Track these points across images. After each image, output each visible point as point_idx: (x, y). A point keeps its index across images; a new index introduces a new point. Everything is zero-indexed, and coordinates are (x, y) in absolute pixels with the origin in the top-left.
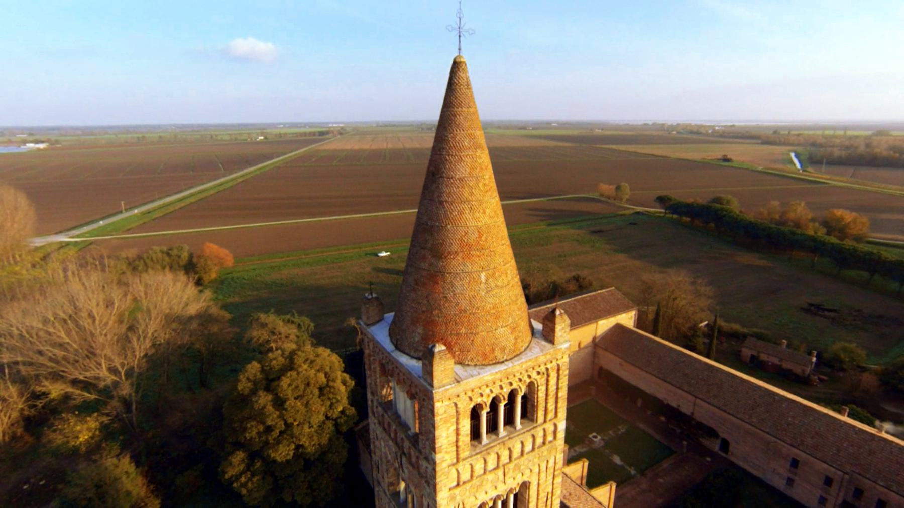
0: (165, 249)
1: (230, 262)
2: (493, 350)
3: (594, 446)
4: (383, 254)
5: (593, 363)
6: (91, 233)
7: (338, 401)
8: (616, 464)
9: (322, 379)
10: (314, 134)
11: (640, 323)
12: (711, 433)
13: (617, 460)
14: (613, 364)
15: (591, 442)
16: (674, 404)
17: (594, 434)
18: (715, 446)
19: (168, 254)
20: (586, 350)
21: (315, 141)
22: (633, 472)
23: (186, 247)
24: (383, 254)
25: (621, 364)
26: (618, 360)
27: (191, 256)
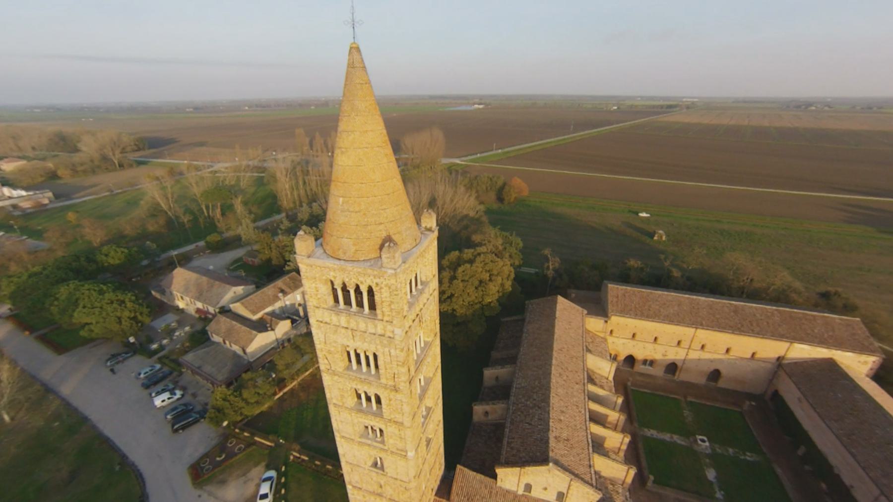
0: (491, 176)
3: (695, 447)
4: (644, 215)
5: (771, 381)
6: (472, 161)
7: (488, 295)
8: (706, 477)
9: (486, 276)
10: (662, 107)
13: (711, 474)
14: (791, 394)
15: (696, 441)
17: (705, 438)
20: (763, 365)
21: (659, 113)
22: (719, 495)
24: (644, 215)
25: (799, 399)
26: (798, 394)
27: (505, 184)
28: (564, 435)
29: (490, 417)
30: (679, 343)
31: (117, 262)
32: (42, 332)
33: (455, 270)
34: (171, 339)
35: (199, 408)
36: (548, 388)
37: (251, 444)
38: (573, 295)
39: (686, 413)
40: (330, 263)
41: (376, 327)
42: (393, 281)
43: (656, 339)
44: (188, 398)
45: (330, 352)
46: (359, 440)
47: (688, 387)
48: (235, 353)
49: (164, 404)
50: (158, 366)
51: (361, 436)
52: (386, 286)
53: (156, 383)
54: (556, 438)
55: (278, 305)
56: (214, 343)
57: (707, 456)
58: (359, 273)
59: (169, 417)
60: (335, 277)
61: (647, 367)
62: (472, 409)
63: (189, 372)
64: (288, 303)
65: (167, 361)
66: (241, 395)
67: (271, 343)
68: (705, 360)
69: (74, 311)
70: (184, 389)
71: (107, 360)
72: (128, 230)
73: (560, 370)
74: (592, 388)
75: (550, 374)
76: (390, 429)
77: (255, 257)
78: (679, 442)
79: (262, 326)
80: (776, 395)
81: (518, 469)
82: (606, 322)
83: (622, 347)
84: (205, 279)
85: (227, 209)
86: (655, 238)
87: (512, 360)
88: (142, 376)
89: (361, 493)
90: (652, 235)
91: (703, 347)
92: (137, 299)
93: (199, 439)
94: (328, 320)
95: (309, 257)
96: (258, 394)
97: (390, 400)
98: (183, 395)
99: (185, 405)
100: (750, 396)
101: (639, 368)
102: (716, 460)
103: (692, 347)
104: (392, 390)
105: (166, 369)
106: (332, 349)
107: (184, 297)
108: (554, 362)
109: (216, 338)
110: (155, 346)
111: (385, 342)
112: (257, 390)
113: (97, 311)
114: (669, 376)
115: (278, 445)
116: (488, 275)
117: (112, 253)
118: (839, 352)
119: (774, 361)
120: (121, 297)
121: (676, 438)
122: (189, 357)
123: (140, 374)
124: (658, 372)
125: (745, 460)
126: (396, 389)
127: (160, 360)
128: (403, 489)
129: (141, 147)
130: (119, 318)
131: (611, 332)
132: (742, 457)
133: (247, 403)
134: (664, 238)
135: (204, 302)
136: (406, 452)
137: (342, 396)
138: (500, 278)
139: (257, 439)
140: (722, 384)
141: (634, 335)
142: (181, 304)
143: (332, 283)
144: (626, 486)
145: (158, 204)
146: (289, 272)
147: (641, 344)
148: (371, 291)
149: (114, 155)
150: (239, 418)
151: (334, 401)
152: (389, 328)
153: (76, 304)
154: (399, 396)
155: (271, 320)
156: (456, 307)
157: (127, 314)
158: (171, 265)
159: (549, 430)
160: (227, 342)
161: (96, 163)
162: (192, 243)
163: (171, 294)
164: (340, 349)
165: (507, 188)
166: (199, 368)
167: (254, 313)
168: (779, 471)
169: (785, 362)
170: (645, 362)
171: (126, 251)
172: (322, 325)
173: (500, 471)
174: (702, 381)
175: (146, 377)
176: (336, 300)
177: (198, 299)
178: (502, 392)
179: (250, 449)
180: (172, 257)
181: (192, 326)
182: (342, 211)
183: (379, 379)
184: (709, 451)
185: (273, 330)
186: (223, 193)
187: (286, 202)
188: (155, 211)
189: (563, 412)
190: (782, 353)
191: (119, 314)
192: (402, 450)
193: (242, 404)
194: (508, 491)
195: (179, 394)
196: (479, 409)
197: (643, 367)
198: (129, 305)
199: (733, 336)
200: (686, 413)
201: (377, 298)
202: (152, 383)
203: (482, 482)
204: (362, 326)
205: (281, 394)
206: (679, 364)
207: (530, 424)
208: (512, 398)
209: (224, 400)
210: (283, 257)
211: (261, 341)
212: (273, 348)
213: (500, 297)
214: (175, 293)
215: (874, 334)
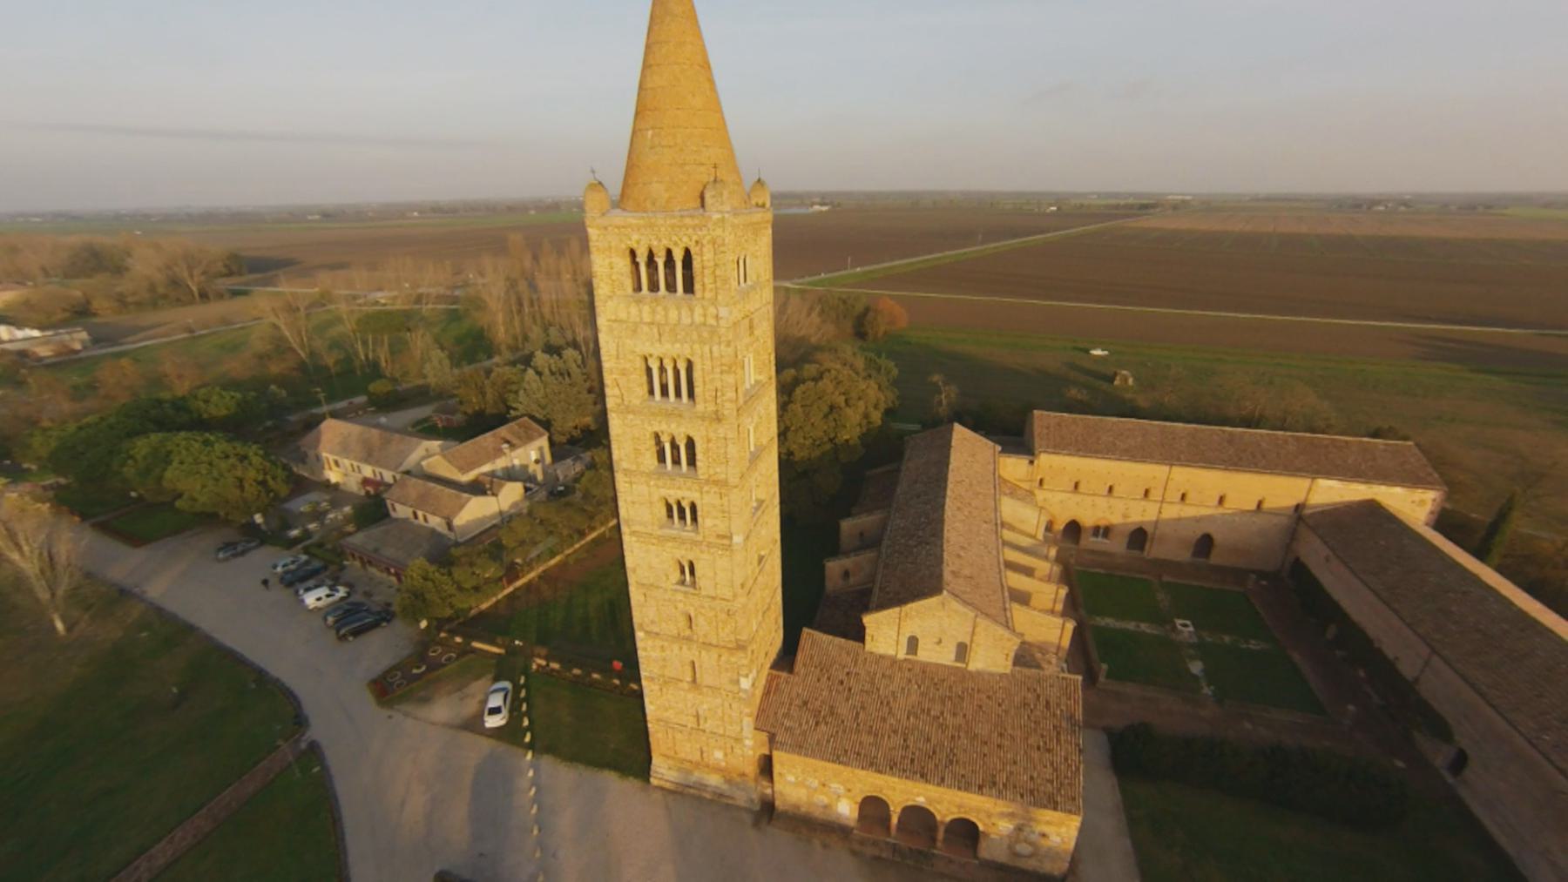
3: (1174, 636)
4: (1097, 352)
5: (1288, 547)
6: (809, 284)
8: (1187, 669)
9: (841, 400)
10: (1131, 207)
12: (1442, 731)
13: (1196, 667)
14: (1314, 554)
15: (1174, 628)
16: (1390, 654)
18: (1440, 758)
19: (844, 302)
20: (1275, 520)
21: (1128, 216)
24: (1097, 352)
25: (1327, 559)
27: (867, 310)
28: (966, 572)
29: (852, 580)
30: (1147, 493)
31: (224, 412)
32: (101, 518)
33: (790, 395)
34: (322, 524)
36: (941, 521)
37: (465, 651)
39: (1160, 596)
41: (692, 310)
42: (719, 232)
43: (1111, 489)
44: (356, 598)
45: (624, 373)
46: (659, 533)
47: (1163, 565)
48: (433, 531)
49: (320, 604)
50: (304, 558)
51: (661, 527)
53: (303, 579)
54: (953, 572)
55: (500, 464)
57: (1192, 646)
58: (673, 226)
59: (330, 619)
62: (823, 567)
63: (357, 563)
64: (517, 462)
66: (450, 574)
67: (492, 517)
69: (165, 470)
70: (346, 585)
71: (220, 550)
75: (943, 506)
76: (707, 499)
77: (453, 412)
79: (478, 488)
80: (1299, 569)
81: (897, 609)
82: (1031, 462)
84: (375, 432)
86: (1117, 382)
88: (279, 569)
89: (659, 643)
90: (1111, 379)
91: (1183, 497)
93: (381, 649)
94: (623, 316)
97: (709, 441)
98: (349, 594)
100: (1262, 574)
101: (1089, 541)
105: (316, 564)
107: (340, 461)
108: (949, 493)
109: (402, 512)
110: (295, 533)
111: (705, 335)
113: (204, 469)
114: (1136, 553)
115: (512, 651)
116: (843, 398)
117: (215, 398)
118: (1383, 488)
119: (1291, 512)
121: (1144, 627)
123: (275, 567)
124: (1117, 546)
126: (718, 418)
127: (306, 551)
128: (723, 616)
129: (234, 268)
130: (241, 480)
131: (1041, 481)
133: (460, 589)
134: (1131, 381)
136: (731, 538)
138: (861, 403)
139: (476, 645)
140: (1215, 559)
141: (1076, 486)
142: (333, 476)
143: (633, 253)
144: (1063, 654)
145: (282, 339)
146: (517, 418)
147: (1089, 500)
149: (191, 276)
150: (448, 612)
151: (625, 465)
153: (167, 460)
155: (492, 483)
156: (794, 447)
157: (252, 474)
160: (420, 514)
161: (161, 290)
162: (342, 399)
163: (318, 458)
165: (871, 315)
166: (376, 550)
167: (463, 470)
168: (1296, 657)
169: (1307, 512)
170: (1096, 530)
171: (238, 395)
172: (615, 325)
173: (869, 620)
174: (1185, 556)
175: (286, 573)
176: (638, 288)
177: (368, 458)
178: (868, 542)
179: (464, 660)
184: (1195, 640)
186: (396, 324)
187: (501, 334)
188: (280, 347)
189: (963, 548)
190: (1300, 498)
191: (239, 473)
192: (723, 537)
194: (882, 657)
195: (342, 592)
196: (834, 567)
197: (1093, 539)
198: (256, 460)
199: (1227, 474)
200: (1160, 596)
201: (696, 264)
202: (297, 580)
203: (841, 648)
204: (673, 314)
205: (511, 589)
206: (1149, 529)
210: (504, 401)
211: (475, 511)
212: (494, 526)
214: (324, 455)
215: (1434, 467)
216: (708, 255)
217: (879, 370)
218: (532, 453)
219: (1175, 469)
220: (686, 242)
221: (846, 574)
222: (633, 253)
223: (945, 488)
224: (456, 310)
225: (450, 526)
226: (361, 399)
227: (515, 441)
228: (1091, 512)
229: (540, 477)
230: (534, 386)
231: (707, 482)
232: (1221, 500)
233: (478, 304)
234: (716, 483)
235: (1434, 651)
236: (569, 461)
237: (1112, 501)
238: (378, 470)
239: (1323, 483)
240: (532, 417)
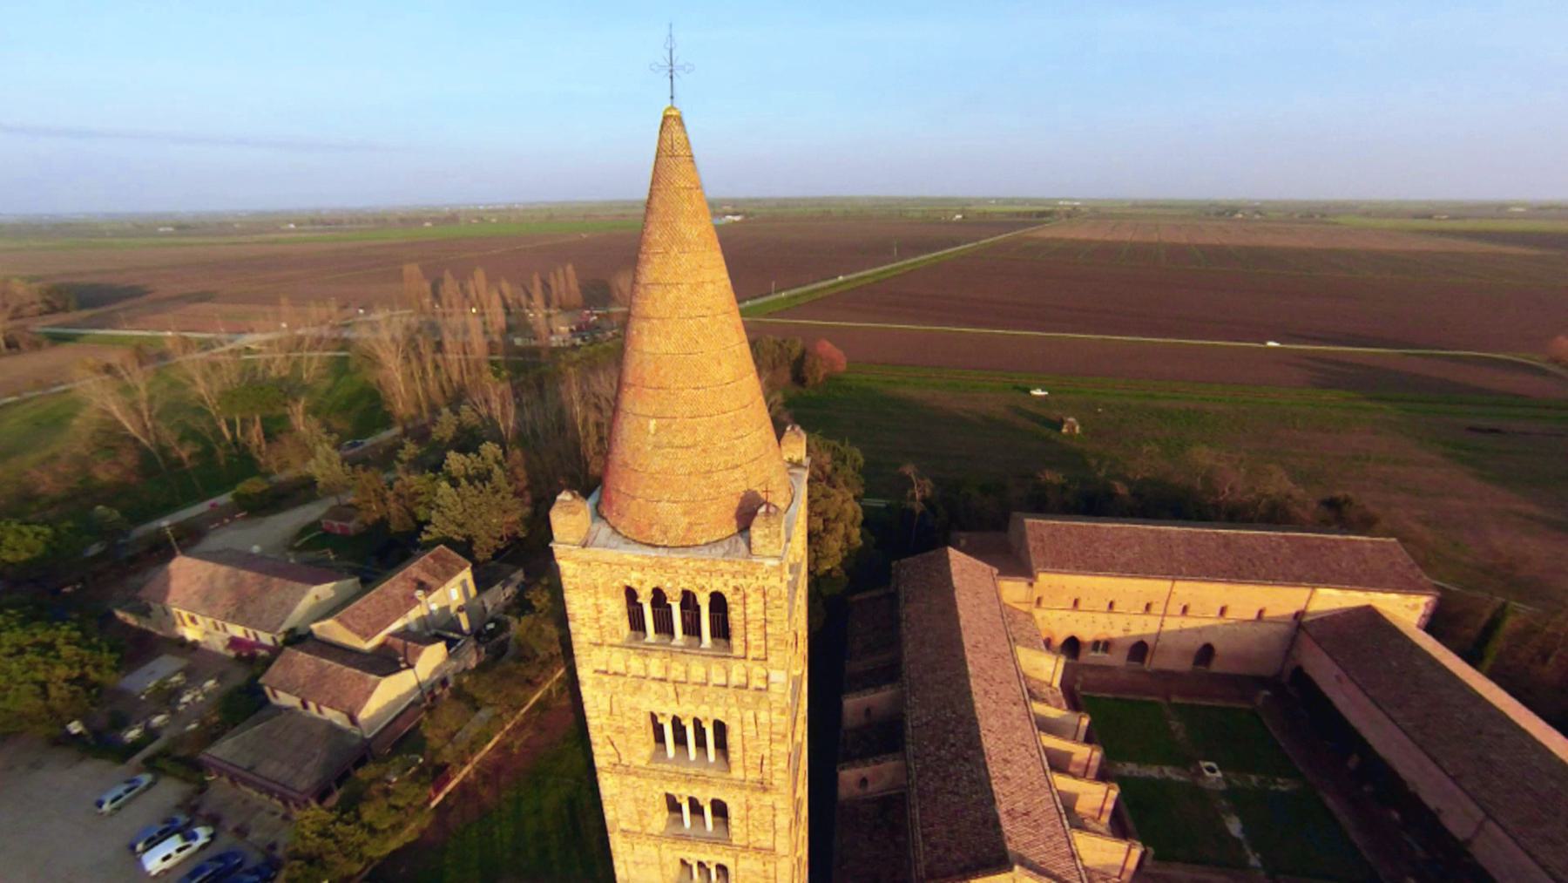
0: (779, 339)
1: (842, 366)
2: (651, 525)
4: (1038, 392)
7: (825, 557)
8: (1226, 831)
10: (1030, 214)
11: (1433, 625)
13: (1234, 826)
14: (1323, 670)
15: (1200, 772)
17: (1214, 765)
20: (1274, 627)
22: (1254, 861)
23: (800, 342)
24: (1038, 392)
26: (1336, 670)
27: (804, 352)
28: (1020, 807)
29: (870, 788)
30: (1148, 607)
31: (24, 556)
34: (174, 712)
35: (255, 859)
36: (974, 722)
38: (963, 542)
39: (1175, 725)
40: (632, 554)
43: (1111, 605)
44: (226, 841)
45: (620, 730)
48: (331, 727)
52: (756, 590)
54: (1008, 813)
55: (414, 614)
56: (280, 710)
58: (698, 571)
60: (642, 583)
61: (1100, 654)
62: (836, 776)
63: (225, 780)
65: (161, 763)
66: (358, 817)
67: (409, 694)
68: (1189, 630)
70: (214, 821)
72: (47, 484)
73: (984, 684)
74: (1038, 708)
76: (743, 864)
77: (349, 518)
78: (1175, 777)
79: (387, 661)
80: (1301, 678)
82: (1031, 585)
83: (1059, 623)
85: (275, 429)
86: (1064, 430)
87: (890, 673)
90: (1058, 425)
91: (1185, 609)
92: (86, 637)
94: (621, 668)
95: (584, 546)
96: (396, 807)
97: (749, 809)
98: (212, 837)
99: (220, 858)
100: (1261, 681)
101: (1088, 657)
102: (1238, 800)
103: (1169, 611)
104: (754, 790)
106: (627, 724)
107: (198, 618)
110: (133, 734)
111: (749, 699)
112: (392, 801)
118: (1379, 595)
119: (1290, 620)
120: (43, 635)
121: (1168, 771)
122: (223, 749)
123: (100, 804)
124: (1117, 659)
125: (1277, 791)
126: (764, 787)
127: (150, 764)
129: (59, 304)
130: (43, 686)
131: (1039, 601)
132: (1273, 788)
133: (373, 830)
135: (246, 623)
137: (642, 814)
138: (841, 526)
140: (1216, 667)
141: (1076, 603)
142: (191, 633)
148: (718, 602)
151: (623, 825)
152: (758, 670)
154: (768, 799)
155: (405, 648)
157: (61, 671)
158: (161, 551)
159: (994, 800)
160: (312, 705)
162: (203, 500)
163: (167, 613)
164: (642, 723)
166: (250, 769)
167: (367, 636)
169: (1307, 619)
170: (1096, 645)
171: (47, 531)
172: (606, 678)
174: (1186, 665)
177: (234, 619)
180: (160, 531)
181: (220, 678)
182: (657, 446)
183: (728, 769)
184: (1223, 786)
185: (410, 666)
186: (266, 395)
187: (401, 406)
188: (111, 438)
189: (1006, 761)
190: (1300, 606)
191: (41, 676)
193: (362, 835)
195: (203, 834)
198: (67, 651)
201: (735, 616)
205: (441, 797)
207: (957, 794)
208: (910, 749)
209: (323, 834)
210: (413, 516)
211: (389, 692)
212: (412, 704)
213: (845, 559)
216: (755, 606)
217: (844, 460)
218: (453, 593)
219: (1178, 584)
220: (717, 585)
221: (864, 782)
222: (631, 594)
223: (963, 662)
224: (346, 358)
225: (352, 719)
226: (225, 499)
227: (431, 581)
228: (1088, 628)
229: (465, 625)
230: (449, 501)
231: (746, 848)
232: (1223, 611)
233: (373, 361)
234: (758, 850)
235: (1489, 816)
236: (498, 587)
237: (1113, 616)
238: (250, 631)
239: (1323, 592)
240: (449, 543)
